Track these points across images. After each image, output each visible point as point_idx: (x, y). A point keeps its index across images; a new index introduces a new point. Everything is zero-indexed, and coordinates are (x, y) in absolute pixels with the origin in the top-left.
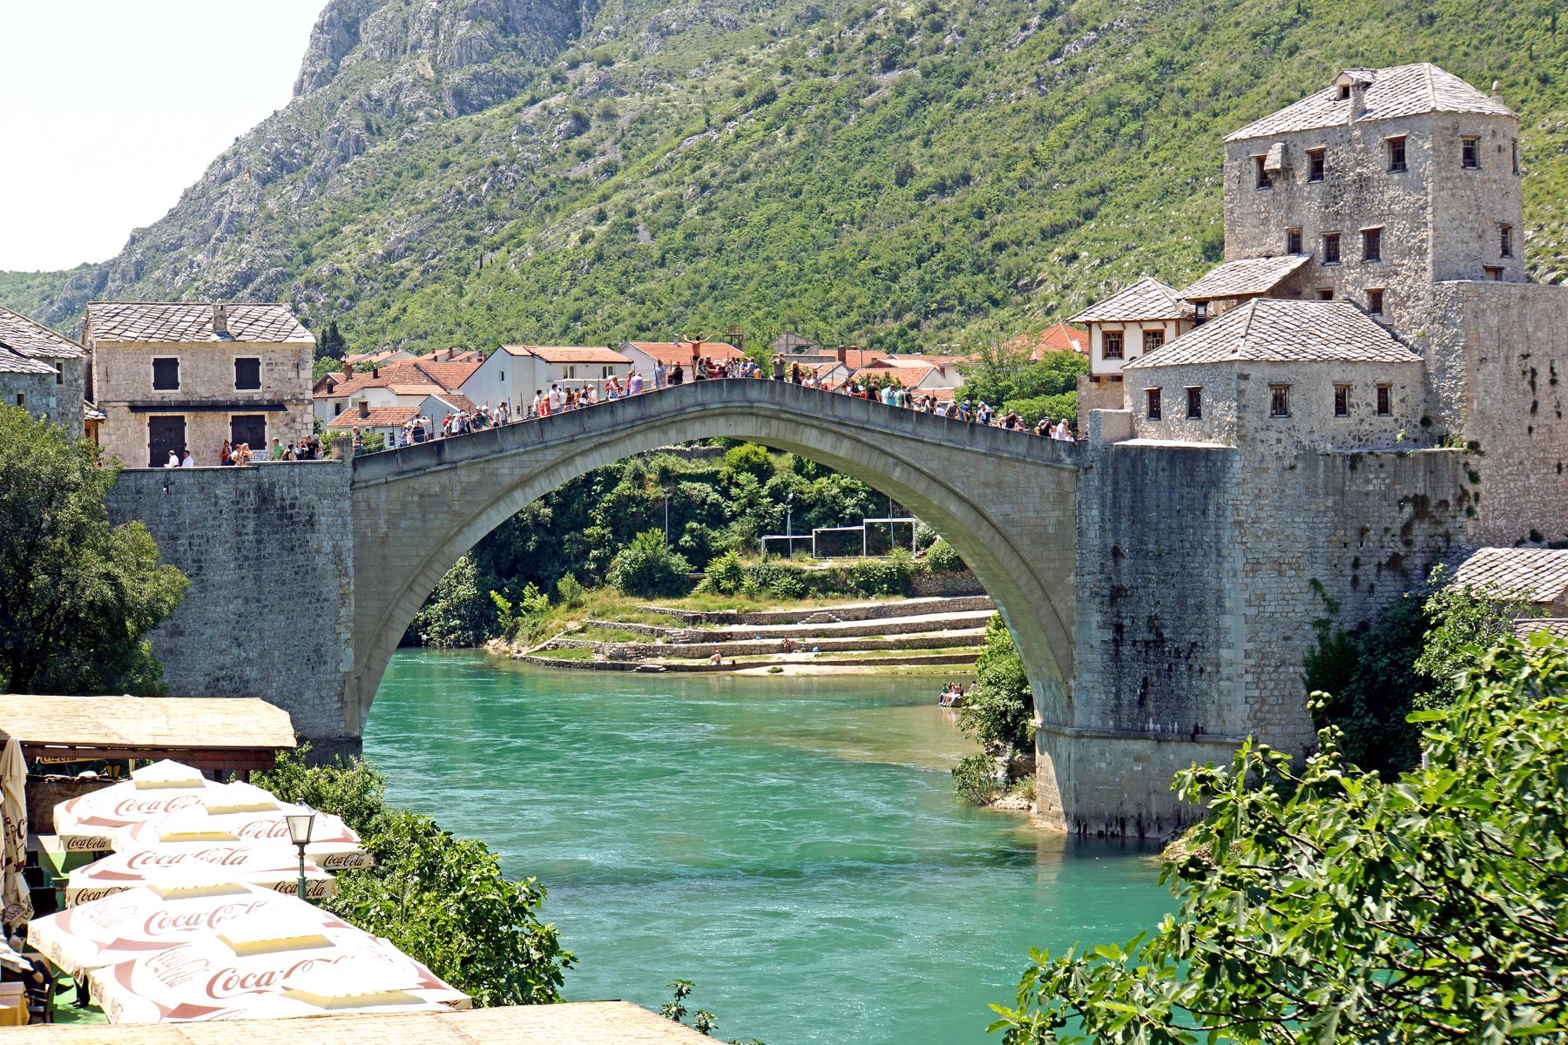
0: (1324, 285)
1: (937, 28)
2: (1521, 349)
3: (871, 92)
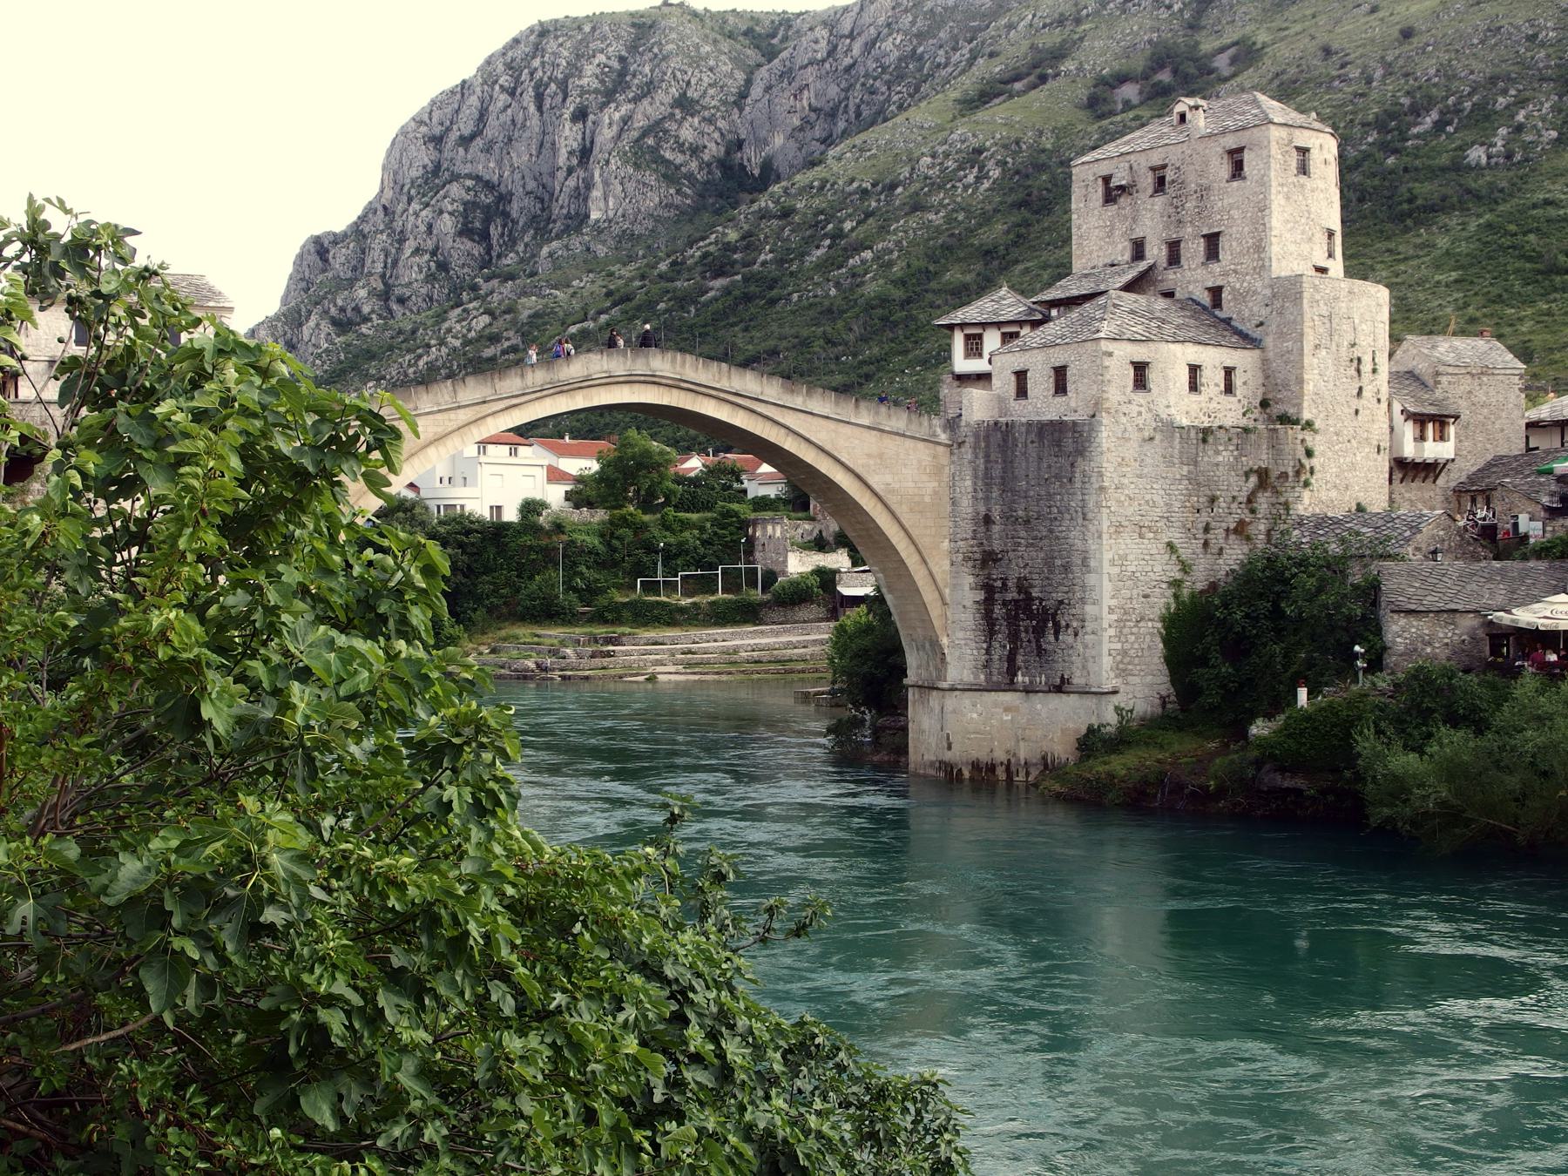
0: (1165, 287)
2: (1349, 337)
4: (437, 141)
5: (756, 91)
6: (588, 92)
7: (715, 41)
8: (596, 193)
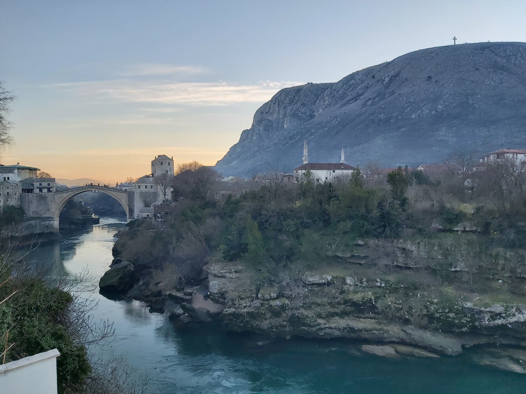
1: (298, 135)
4: (262, 113)
5: (318, 101)
6: (287, 103)
8: (285, 123)
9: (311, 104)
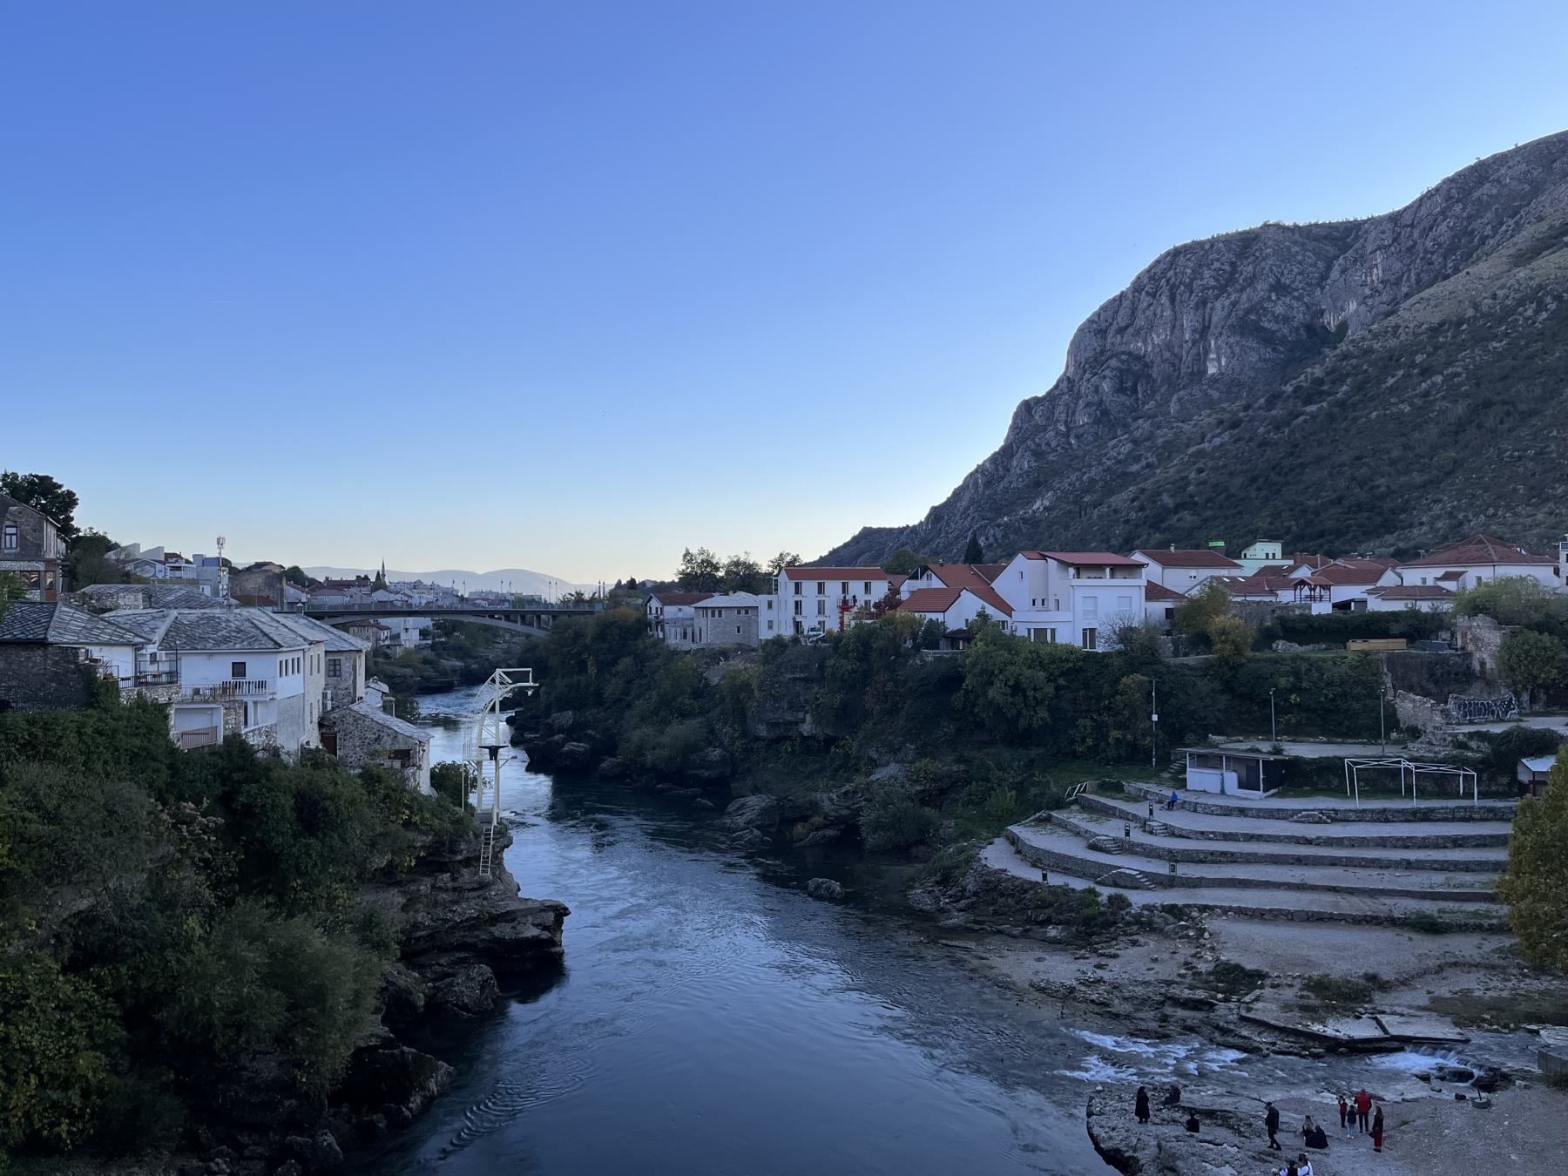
1: (1341, 380)
3: (1297, 417)
5: (1335, 274)
7: (1303, 245)
8: (1212, 356)
9: (1309, 285)
